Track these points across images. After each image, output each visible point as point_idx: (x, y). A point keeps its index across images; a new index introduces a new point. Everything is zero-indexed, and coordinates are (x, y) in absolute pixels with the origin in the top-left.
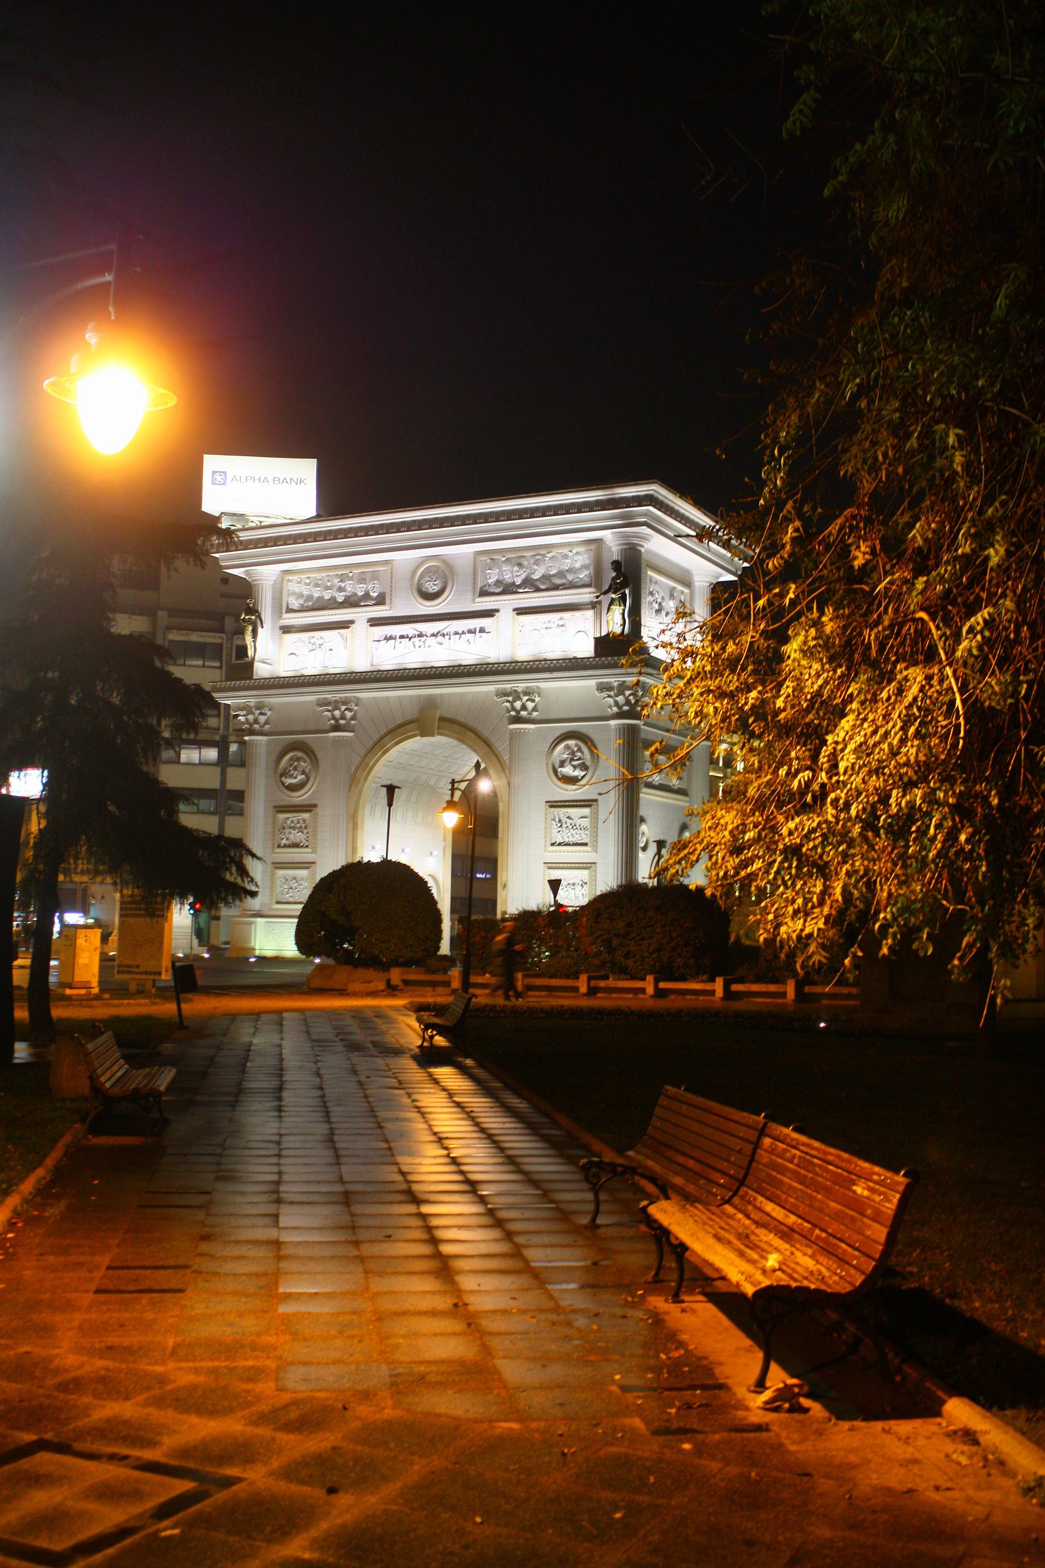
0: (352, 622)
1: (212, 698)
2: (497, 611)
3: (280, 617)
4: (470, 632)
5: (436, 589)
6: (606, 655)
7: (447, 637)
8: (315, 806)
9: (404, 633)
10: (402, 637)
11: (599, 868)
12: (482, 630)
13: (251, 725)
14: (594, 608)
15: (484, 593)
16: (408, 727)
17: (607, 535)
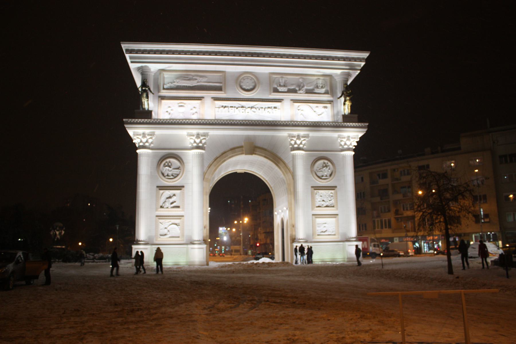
0: (203, 97)
1: (125, 128)
2: (283, 100)
3: (159, 91)
4: (269, 108)
5: (251, 87)
6: (347, 122)
7: (258, 109)
8: (183, 187)
9: (233, 106)
10: (231, 107)
11: (339, 217)
12: (275, 108)
13: (144, 143)
14: (330, 103)
15: (276, 91)
16: (236, 150)
17: (339, 72)
